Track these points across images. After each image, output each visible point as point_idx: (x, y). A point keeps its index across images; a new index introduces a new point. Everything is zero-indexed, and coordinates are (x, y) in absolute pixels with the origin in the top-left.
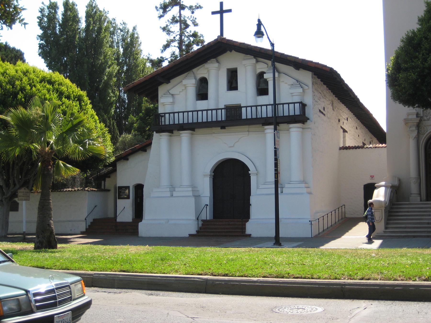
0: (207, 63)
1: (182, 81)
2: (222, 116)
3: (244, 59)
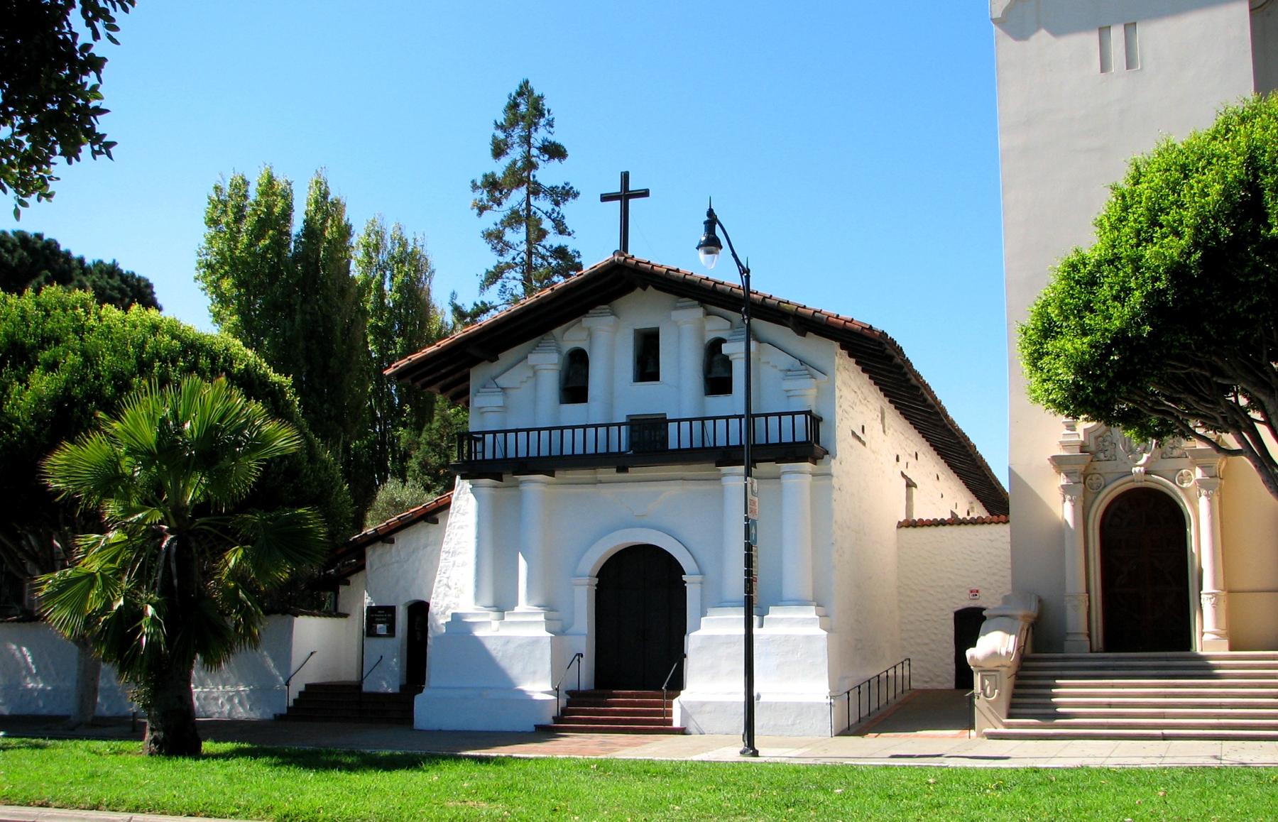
1: (527, 358)
2: (620, 440)
3: (676, 308)
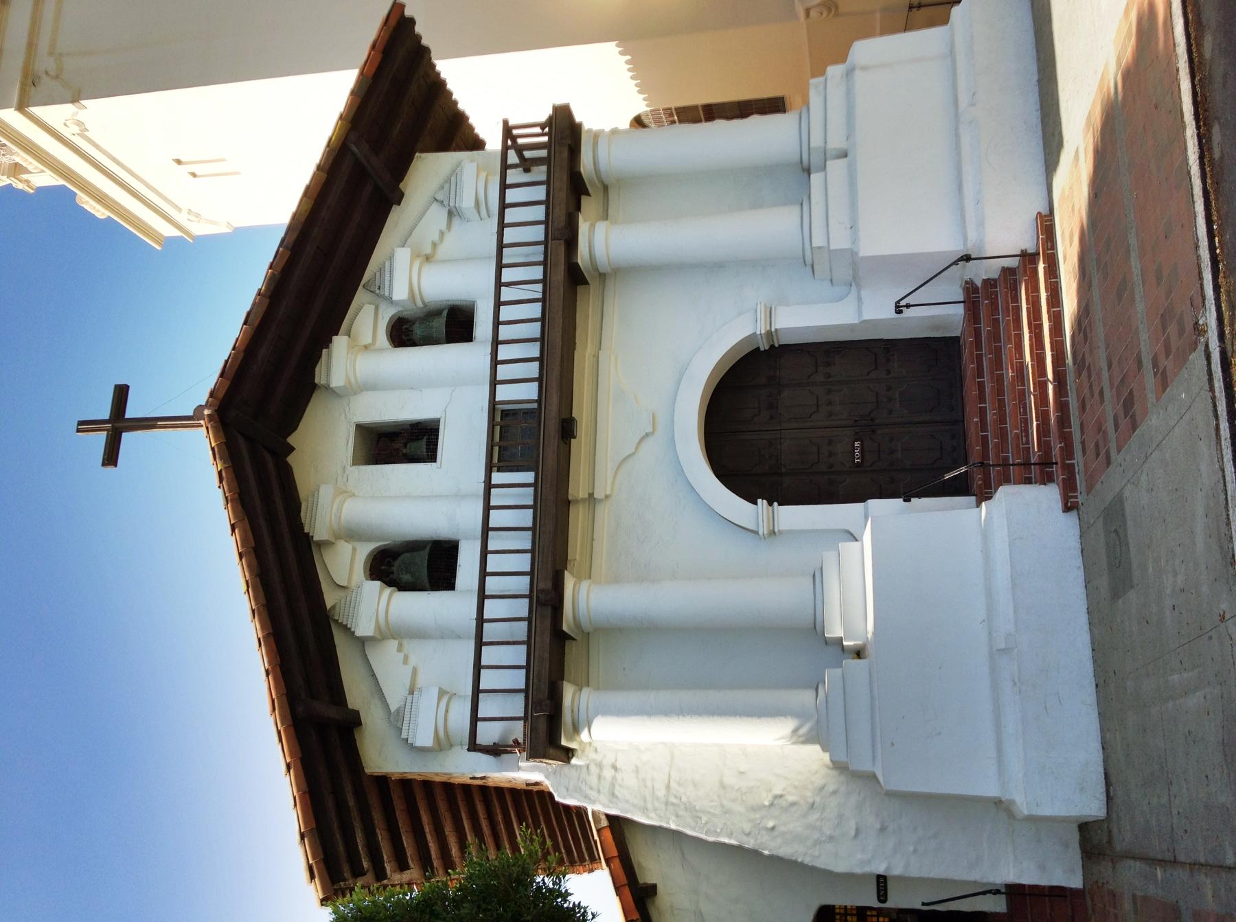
0: (311, 534)
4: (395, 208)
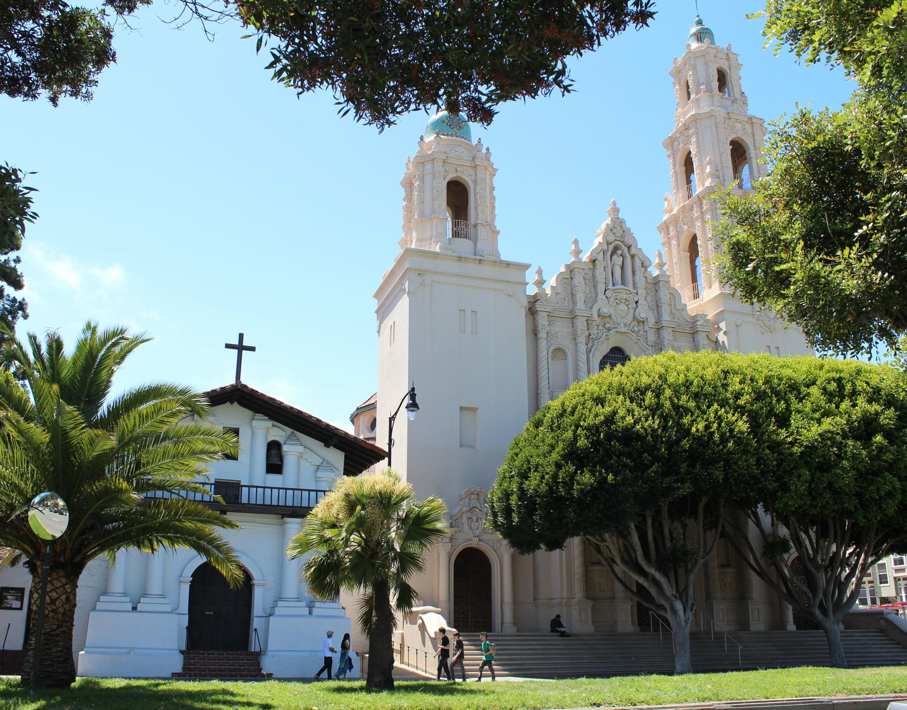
3: (253, 419)
4: (323, 444)
